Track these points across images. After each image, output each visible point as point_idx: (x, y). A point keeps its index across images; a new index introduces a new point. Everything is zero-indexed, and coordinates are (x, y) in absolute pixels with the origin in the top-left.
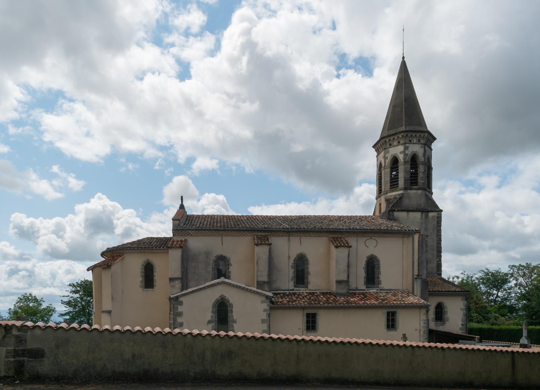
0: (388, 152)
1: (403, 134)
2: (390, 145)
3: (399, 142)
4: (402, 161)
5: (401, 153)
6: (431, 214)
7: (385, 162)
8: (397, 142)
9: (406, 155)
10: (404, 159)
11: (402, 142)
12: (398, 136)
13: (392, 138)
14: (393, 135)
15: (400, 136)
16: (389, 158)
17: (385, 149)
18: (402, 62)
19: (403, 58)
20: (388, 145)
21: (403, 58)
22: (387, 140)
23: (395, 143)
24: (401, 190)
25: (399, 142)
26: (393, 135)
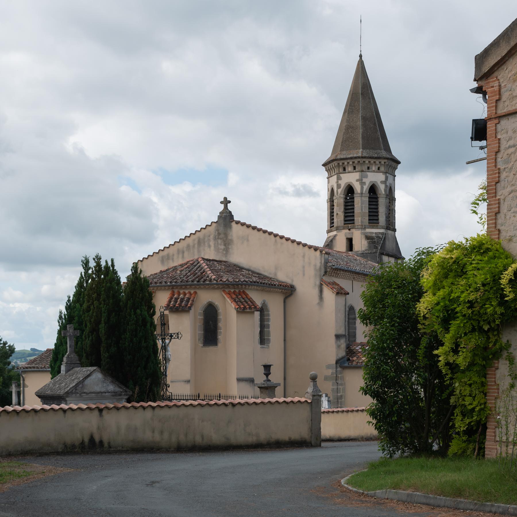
0: (366, 177)
1: (386, 161)
2: (368, 168)
3: (379, 168)
4: (384, 193)
5: (382, 182)
6: (399, 261)
7: (362, 188)
8: (377, 168)
9: (386, 186)
10: (385, 191)
11: (382, 169)
12: (380, 160)
13: (372, 161)
14: (376, 158)
15: (383, 163)
16: (367, 184)
17: (362, 171)
18: (359, 61)
19: (361, 56)
20: (365, 168)
21: (361, 56)
22: (367, 162)
23: (374, 168)
24: (382, 228)
25: (379, 168)
26: (376, 158)
